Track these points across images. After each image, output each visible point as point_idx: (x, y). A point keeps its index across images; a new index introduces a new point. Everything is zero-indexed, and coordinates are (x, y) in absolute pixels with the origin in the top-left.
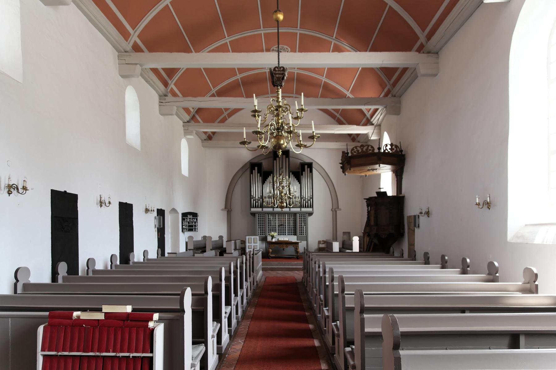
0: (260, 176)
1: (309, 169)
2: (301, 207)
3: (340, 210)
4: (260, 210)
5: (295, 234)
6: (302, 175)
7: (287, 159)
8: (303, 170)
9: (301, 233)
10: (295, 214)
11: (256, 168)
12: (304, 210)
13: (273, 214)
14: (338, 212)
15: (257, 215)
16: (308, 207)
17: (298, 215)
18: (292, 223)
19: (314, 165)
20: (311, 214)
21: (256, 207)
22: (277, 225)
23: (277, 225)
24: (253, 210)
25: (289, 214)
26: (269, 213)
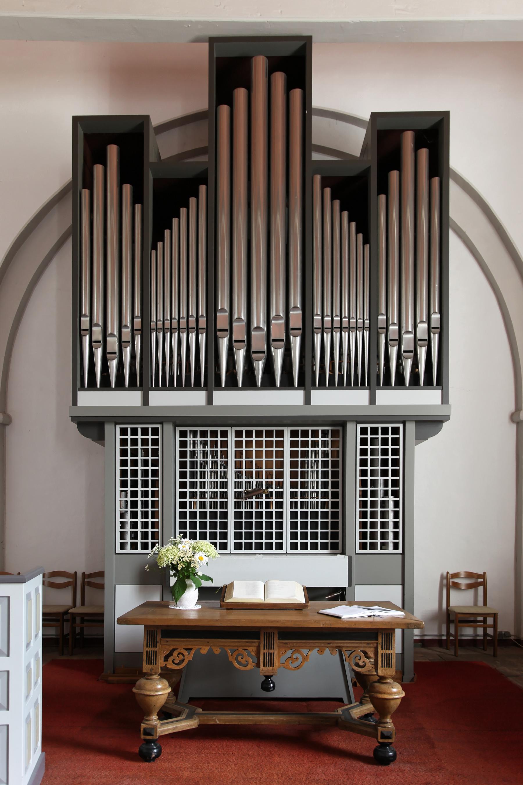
0: (138, 197)
4: (129, 399)
5: (336, 546)
6: (383, 188)
7: (297, 93)
10: (337, 425)
11: (113, 152)
12: (390, 399)
13: (211, 426)
15: (114, 434)
16: (415, 383)
17: (353, 433)
18: (314, 480)
20: (429, 424)
21: (106, 385)
22: (231, 490)
23: (231, 490)
24: (91, 400)
25: (301, 424)
26: (184, 423)
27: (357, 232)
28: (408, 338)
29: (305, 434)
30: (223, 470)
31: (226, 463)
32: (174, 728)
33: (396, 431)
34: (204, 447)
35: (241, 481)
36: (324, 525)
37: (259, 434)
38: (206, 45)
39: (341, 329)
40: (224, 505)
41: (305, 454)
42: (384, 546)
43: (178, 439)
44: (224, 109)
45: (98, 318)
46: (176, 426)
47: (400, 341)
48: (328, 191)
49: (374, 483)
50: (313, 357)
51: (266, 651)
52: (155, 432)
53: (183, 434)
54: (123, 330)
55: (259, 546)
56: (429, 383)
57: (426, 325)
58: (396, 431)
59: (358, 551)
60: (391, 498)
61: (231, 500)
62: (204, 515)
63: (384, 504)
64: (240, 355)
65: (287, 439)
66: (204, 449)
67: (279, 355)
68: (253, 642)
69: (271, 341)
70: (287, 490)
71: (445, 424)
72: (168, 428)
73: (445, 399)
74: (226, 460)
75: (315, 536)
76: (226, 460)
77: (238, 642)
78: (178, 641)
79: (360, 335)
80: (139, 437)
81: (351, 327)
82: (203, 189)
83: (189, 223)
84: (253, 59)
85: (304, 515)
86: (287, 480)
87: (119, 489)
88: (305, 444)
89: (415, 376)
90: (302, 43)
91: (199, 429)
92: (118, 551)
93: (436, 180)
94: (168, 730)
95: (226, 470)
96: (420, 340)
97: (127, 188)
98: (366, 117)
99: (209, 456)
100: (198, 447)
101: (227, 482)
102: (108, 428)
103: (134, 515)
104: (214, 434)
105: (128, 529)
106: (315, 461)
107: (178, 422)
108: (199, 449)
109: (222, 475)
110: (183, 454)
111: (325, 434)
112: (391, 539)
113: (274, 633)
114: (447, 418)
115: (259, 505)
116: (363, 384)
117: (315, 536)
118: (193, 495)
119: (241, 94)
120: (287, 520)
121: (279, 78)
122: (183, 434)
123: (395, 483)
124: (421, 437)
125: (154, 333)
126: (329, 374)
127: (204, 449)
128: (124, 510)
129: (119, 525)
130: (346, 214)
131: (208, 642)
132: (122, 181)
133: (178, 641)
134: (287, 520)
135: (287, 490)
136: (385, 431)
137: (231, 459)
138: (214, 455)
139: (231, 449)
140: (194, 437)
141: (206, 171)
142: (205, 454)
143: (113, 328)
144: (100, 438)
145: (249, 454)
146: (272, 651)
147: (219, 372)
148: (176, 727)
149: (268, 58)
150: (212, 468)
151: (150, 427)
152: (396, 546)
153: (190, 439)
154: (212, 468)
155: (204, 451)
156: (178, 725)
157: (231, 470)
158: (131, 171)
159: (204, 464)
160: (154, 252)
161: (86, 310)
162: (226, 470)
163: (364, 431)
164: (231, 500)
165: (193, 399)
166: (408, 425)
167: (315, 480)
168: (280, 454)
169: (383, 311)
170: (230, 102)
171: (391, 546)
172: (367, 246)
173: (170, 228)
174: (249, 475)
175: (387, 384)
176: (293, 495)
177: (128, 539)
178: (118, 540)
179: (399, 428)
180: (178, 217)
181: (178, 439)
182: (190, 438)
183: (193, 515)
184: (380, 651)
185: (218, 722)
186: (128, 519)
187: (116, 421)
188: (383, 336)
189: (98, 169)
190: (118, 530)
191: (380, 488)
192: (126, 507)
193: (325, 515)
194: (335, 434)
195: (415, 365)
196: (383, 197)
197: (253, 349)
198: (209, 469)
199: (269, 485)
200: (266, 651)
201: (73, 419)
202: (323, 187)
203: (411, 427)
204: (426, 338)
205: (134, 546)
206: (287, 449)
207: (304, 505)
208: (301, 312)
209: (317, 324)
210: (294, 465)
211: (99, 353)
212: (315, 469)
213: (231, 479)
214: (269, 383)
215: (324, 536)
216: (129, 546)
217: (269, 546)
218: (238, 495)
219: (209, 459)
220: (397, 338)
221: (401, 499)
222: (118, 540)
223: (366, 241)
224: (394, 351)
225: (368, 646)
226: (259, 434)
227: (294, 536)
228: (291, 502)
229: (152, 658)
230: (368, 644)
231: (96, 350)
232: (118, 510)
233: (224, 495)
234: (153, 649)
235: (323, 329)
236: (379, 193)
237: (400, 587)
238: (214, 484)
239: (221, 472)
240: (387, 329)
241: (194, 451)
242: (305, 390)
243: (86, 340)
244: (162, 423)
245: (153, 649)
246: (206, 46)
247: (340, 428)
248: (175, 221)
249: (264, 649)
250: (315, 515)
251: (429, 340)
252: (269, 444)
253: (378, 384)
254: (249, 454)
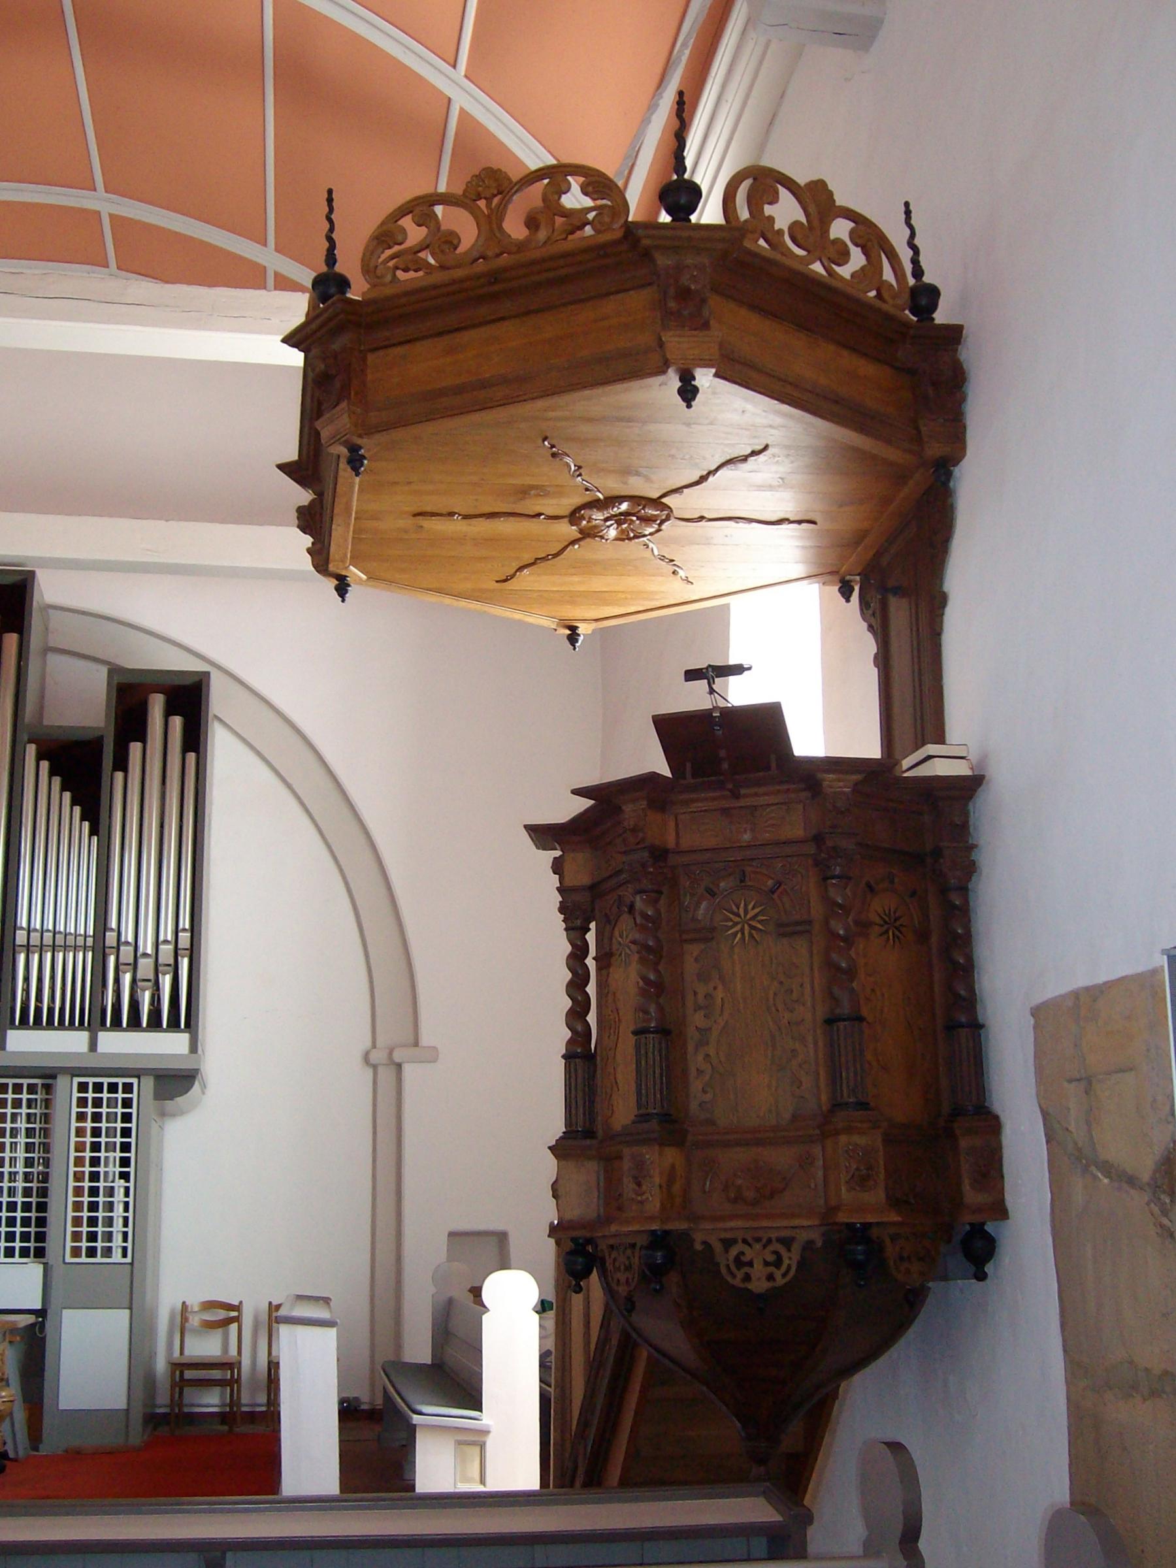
1: (177, 722)
2: (96, 1019)
3: (432, 1056)
6: (121, 763)
9: (92, 1243)
12: (117, 1044)
14: (407, 1069)
16: (155, 1023)
17: (67, 1091)
19: (220, 701)
20: (175, 1082)
33: (128, 1088)
39: (54, 948)
42: (108, 1252)
48: (45, 765)
56: (174, 1025)
59: (69, 1259)
63: (110, 1192)
89: (155, 1013)
130: (67, 796)
169: (114, 925)
175: (117, 1024)
179: (132, 1084)
188: (112, 959)
196: (119, 775)
203: (148, 1083)
223: (94, 831)
224: (127, 978)
235: (28, 948)
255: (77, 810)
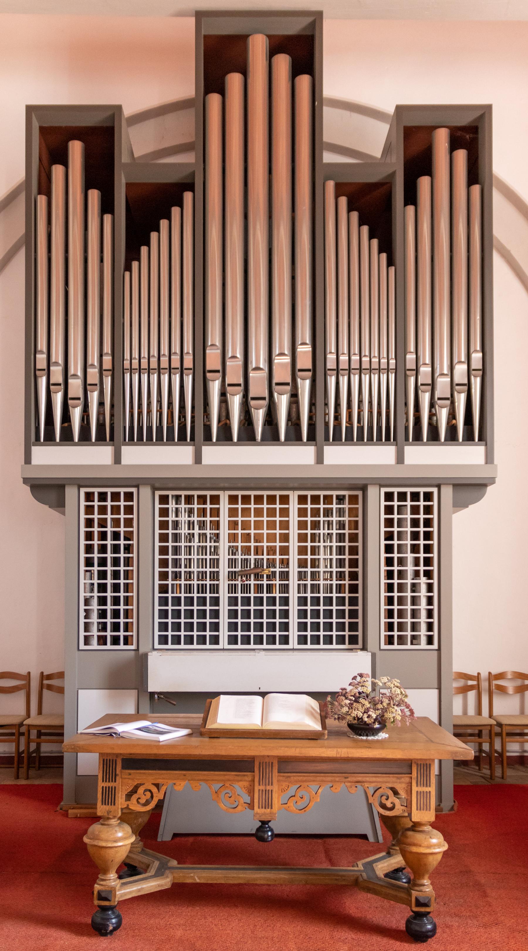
0: (107, 206)
6: (411, 198)
7: (304, 80)
8: (419, 164)
11: (76, 150)
17: (376, 499)
18: (327, 557)
20: (470, 489)
22: (224, 569)
23: (224, 569)
26: (165, 487)
27: (380, 251)
28: (443, 382)
29: (315, 499)
30: (213, 544)
31: (217, 535)
32: (139, 890)
33: (428, 497)
34: (189, 516)
35: (235, 559)
36: (341, 614)
37: (259, 499)
38: (193, 20)
40: (215, 589)
41: (316, 525)
43: (157, 506)
44: (215, 99)
45: (58, 355)
46: (154, 489)
47: (433, 385)
48: (343, 201)
49: (402, 562)
50: (326, 405)
51: (262, 787)
52: (129, 496)
53: (164, 499)
54: (90, 370)
55: (259, 640)
56: (469, 437)
57: (465, 367)
58: (428, 497)
59: (383, 647)
60: (423, 581)
61: (224, 583)
62: (190, 601)
63: (415, 587)
64: (236, 402)
65: (294, 506)
66: (190, 519)
67: (283, 402)
68: (244, 775)
69: (274, 385)
70: (294, 569)
71: (489, 489)
72: (146, 492)
73: (489, 458)
74: (217, 532)
75: (329, 627)
76: (217, 532)
77: (225, 775)
78: (144, 773)
79: (384, 377)
80: (109, 503)
81: (372, 367)
82: (188, 197)
83: (171, 236)
84: (250, 38)
85: (316, 601)
86: (294, 557)
87: (83, 568)
88: (316, 513)
90: (310, 19)
91: (183, 493)
92: (82, 646)
93: (476, 189)
94: (130, 892)
95: (216, 544)
96: (458, 385)
97: (94, 195)
98: (391, 110)
99: (196, 527)
100: (182, 516)
101: (218, 560)
102: (70, 493)
103: (102, 601)
104: (202, 499)
105: (95, 619)
106: (328, 534)
107: (157, 485)
108: (183, 518)
109: (213, 550)
110: (164, 525)
111: (340, 499)
112: (423, 632)
113: (272, 763)
114: (492, 481)
115: (259, 588)
116: (388, 438)
117: (329, 627)
118: (177, 576)
119: (234, 81)
120: (294, 608)
121: (283, 62)
122: (164, 499)
123: (428, 562)
124: (460, 504)
125: (128, 374)
126: (346, 427)
127: (190, 519)
128: (88, 595)
129: (82, 614)
130: (365, 229)
131: (185, 775)
132: (88, 185)
133: (144, 773)
134: (294, 608)
135: (294, 569)
136: (415, 496)
137: (224, 531)
138: (202, 525)
139: (224, 519)
140: (177, 504)
141: (193, 175)
142: (191, 525)
143: (76, 367)
144: (59, 504)
145: (246, 525)
146: (269, 788)
147: (208, 423)
148: (142, 888)
149: (270, 37)
150: (199, 542)
151: (122, 490)
152: (430, 640)
153: (172, 505)
154: (199, 542)
155: (189, 521)
156: (144, 886)
157: (224, 544)
158: (100, 173)
159: (190, 537)
160: (127, 274)
161: (42, 345)
162: (216, 544)
163: (389, 497)
164: (224, 583)
165: (175, 457)
166: (444, 489)
167: (329, 557)
168: (285, 525)
169: (412, 348)
170: (222, 91)
171: (424, 640)
172: (392, 269)
173: (148, 244)
174: (247, 550)
175: (418, 437)
176: (302, 576)
177: (95, 632)
178: (82, 634)
180: (158, 230)
181: (157, 506)
182: (172, 504)
183: (177, 601)
184: (415, 789)
185: (198, 881)
186: (95, 606)
187: (80, 483)
188: (412, 380)
189: (58, 170)
190: (82, 620)
191: (410, 568)
192: (92, 591)
193: (341, 601)
194: (353, 499)
195: (452, 415)
196: (411, 209)
197: (251, 394)
198: (195, 543)
199: (271, 563)
200: (262, 787)
201: (26, 481)
202: (337, 196)
203: (447, 492)
204: (466, 382)
205: (102, 640)
206: (294, 519)
207: (315, 588)
208: (311, 349)
209: (331, 364)
210: (302, 538)
211: (58, 399)
212: (329, 544)
213: (224, 557)
214: (272, 435)
215: (341, 627)
216: (95, 641)
217: (272, 640)
218: (232, 576)
219: (196, 531)
220: (430, 382)
221: (435, 581)
222: (82, 634)
223: (390, 262)
224: (425, 399)
225: (398, 781)
226: (259, 499)
227: (302, 627)
228: (299, 585)
229: (110, 796)
230: (398, 778)
231: (55, 394)
232: (82, 595)
233: (215, 576)
234: (111, 784)
236: (406, 204)
237: (436, 692)
238: (202, 563)
239: (210, 547)
240: (417, 370)
241: (177, 521)
242: (316, 445)
243: (43, 382)
244: (137, 486)
245: (111, 784)
246: (192, 21)
247: (360, 493)
248: (154, 236)
249: (259, 785)
250: (329, 601)
251: (469, 385)
252: (271, 513)
253: (407, 439)
254: (246, 525)
255: (375, 242)
